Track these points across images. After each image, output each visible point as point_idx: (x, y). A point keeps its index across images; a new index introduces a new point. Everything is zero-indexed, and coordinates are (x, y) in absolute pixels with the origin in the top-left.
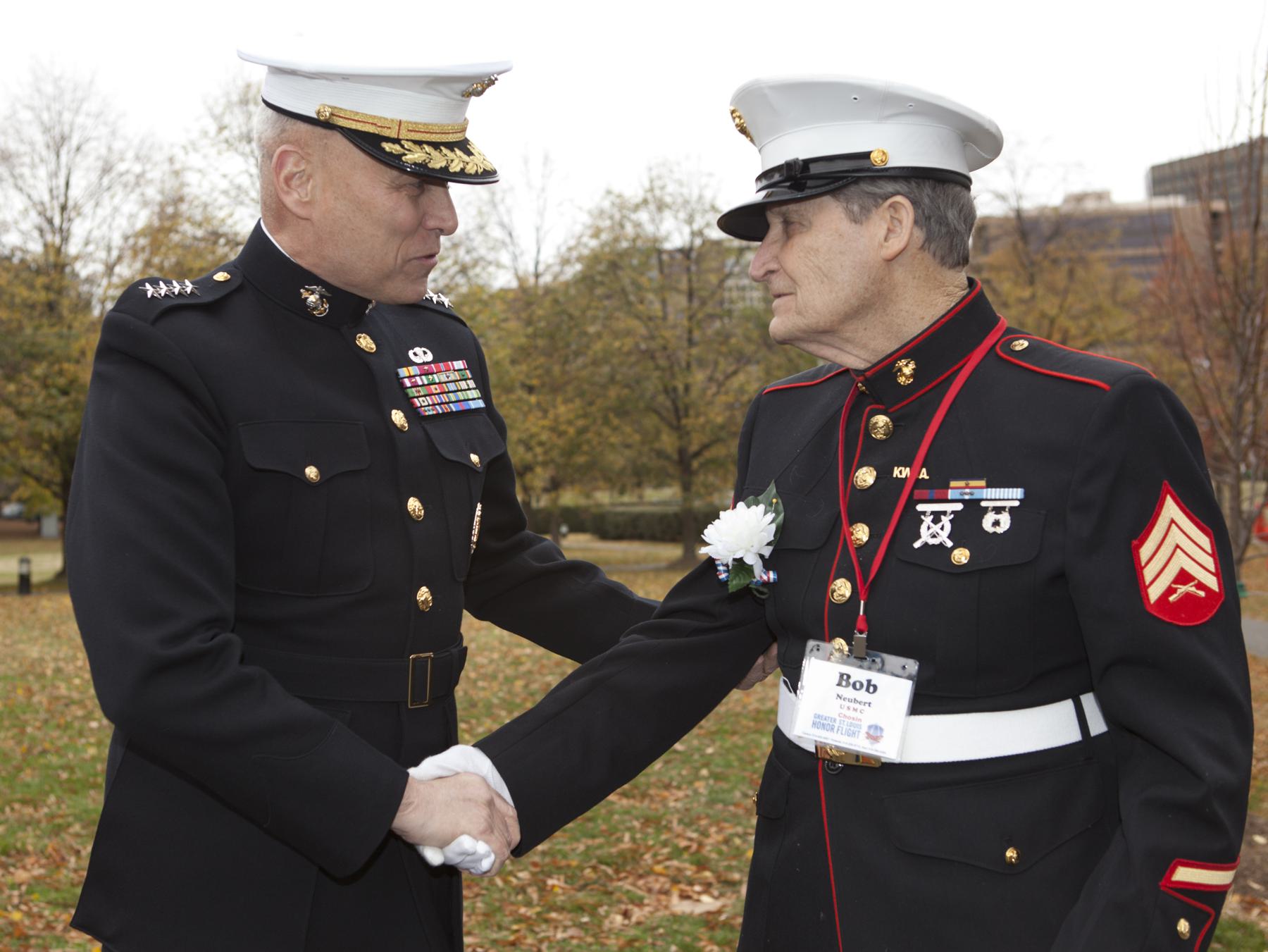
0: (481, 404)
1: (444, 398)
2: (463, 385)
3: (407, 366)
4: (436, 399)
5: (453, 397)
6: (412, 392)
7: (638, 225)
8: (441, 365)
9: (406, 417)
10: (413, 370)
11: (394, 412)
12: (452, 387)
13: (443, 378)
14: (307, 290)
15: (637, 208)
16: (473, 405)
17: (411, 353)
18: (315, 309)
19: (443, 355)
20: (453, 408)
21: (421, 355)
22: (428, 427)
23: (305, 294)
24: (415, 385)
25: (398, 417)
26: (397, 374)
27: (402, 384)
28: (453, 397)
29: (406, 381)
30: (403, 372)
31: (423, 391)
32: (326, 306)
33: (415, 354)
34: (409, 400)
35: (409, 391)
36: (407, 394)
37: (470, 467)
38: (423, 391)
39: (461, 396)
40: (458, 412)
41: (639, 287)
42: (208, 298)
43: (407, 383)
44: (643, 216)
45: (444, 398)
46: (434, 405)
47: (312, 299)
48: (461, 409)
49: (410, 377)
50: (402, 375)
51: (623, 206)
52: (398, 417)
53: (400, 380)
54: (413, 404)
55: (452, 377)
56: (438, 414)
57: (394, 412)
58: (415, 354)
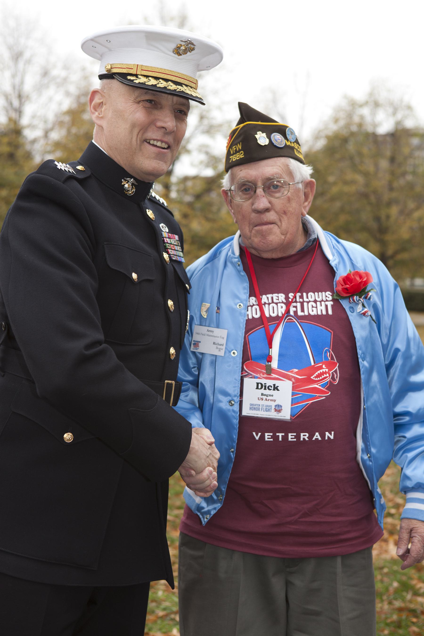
7: (362, 117)
15: (361, 106)
23: (124, 182)
41: (360, 154)
44: (366, 111)
47: (126, 186)
51: (354, 105)
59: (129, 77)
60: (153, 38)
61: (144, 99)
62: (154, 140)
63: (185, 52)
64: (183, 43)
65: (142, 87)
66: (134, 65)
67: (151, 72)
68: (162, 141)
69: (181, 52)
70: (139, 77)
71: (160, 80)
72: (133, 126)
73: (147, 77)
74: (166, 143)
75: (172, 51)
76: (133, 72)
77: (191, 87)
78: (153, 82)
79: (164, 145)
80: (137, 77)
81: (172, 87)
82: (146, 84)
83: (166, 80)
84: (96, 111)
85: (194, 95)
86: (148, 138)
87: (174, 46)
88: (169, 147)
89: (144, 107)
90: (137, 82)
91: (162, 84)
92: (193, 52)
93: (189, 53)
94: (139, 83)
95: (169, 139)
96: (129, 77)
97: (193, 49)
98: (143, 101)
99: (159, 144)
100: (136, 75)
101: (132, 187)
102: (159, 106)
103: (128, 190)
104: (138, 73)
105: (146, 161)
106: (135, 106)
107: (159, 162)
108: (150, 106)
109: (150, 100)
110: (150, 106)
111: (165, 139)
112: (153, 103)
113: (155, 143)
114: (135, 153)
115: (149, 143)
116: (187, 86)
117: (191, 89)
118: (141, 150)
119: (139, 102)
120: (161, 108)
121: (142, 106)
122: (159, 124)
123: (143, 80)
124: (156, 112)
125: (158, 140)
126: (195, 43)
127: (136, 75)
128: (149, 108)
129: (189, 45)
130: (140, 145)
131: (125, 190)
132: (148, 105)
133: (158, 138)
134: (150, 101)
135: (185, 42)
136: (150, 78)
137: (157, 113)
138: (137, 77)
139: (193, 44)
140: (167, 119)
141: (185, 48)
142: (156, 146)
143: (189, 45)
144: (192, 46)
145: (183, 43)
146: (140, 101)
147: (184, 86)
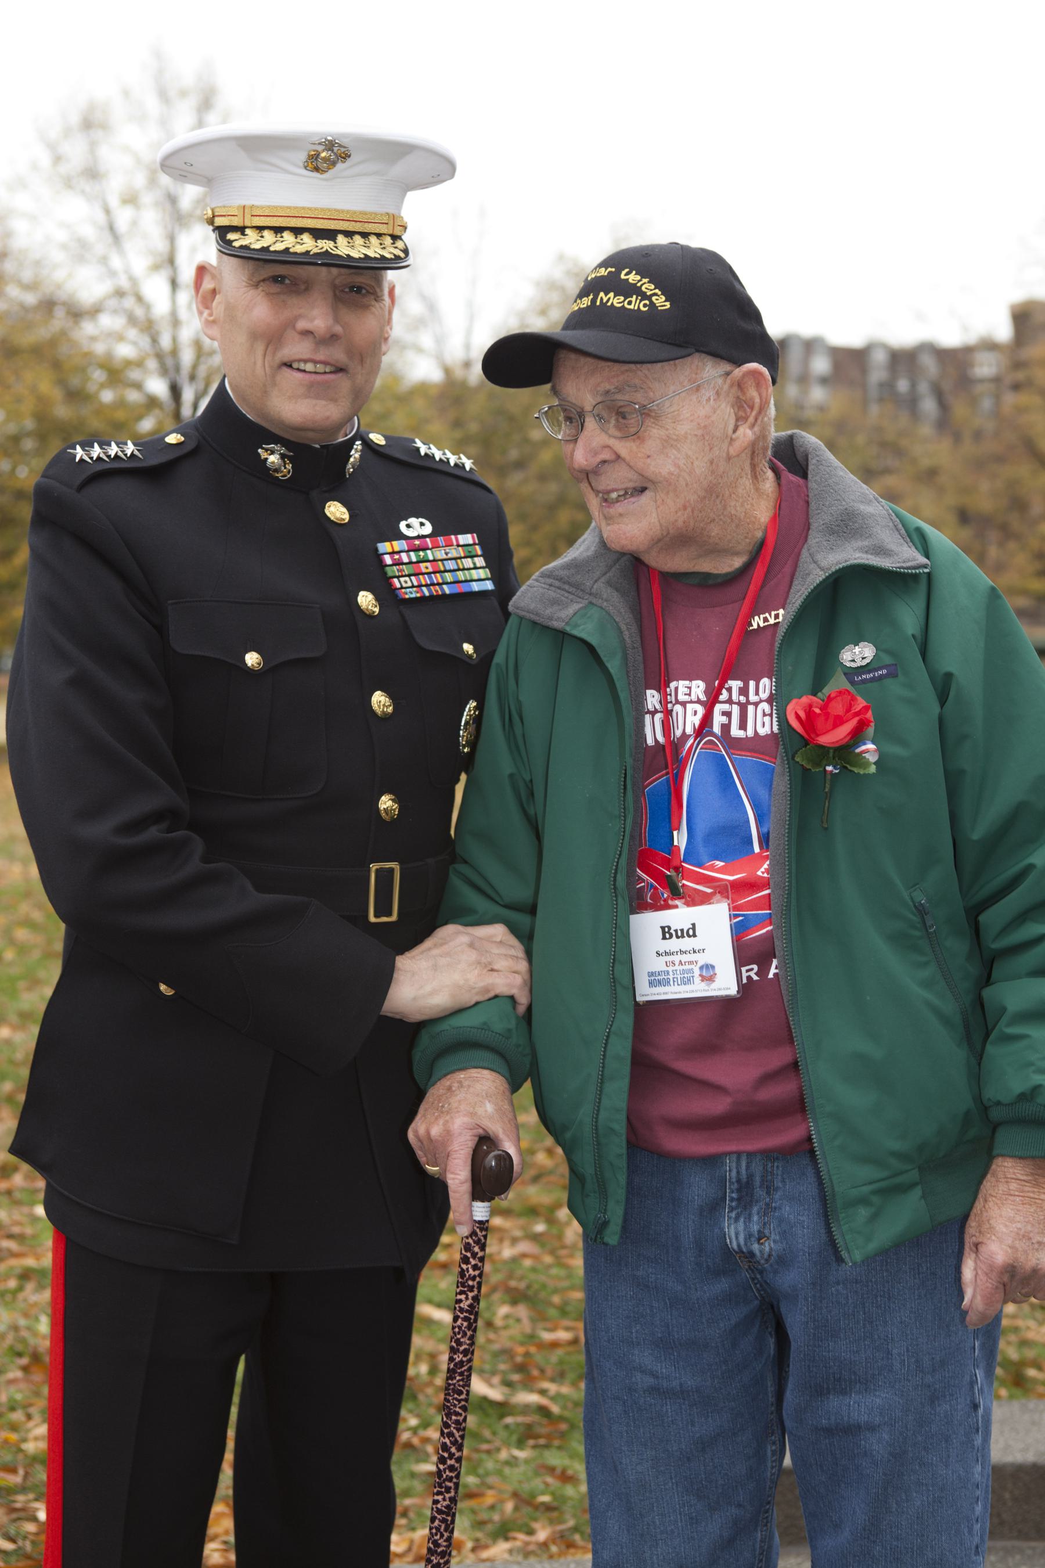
0: (489, 586)
2: (468, 563)
5: (449, 577)
9: (377, 599)
10: (398, 545)
12: (451, 565)
13: (440, 554)
16: (476, 587)
19: (444, 528)
20: (447, 589)
24: (399, 563)
25: (366, 600)
26: (377, 550)
28: (449, 577)
30: (384, 547)
31: (406, 570)
34: (387, 580)
35: (387, 568)
36: (386, 573)
38: (406, 570)
39: (461, 576)
40: (452, 596)
43: (388, 560)
52: (366, 600)
53: (379, 557)
54: (391, 585)
55: (453, 553)
59: (231, 236)
60: (258, 147)
61: (265, 276)
62: (299, 361)
64: (320, 148)
66: (238, 208)
67: (268, 219)
70: (248, 231)
72: (254, 336)
73: (260, 229)
74: (325, 363)
75: (301, 165)
76: (236, 222)
77: (365, 235)
78: (269, 239)
79: (320, 368)
80: (243, 234)
82: (252, 247)
83: (297, 231)
86: (286, 360)
87: (302, 156)
88: (340, 370)
89: (268, 294)
90: (236, 244)
91: (288, 240)
93: (340, 166)
94: (241, 247)
95: (338, 354)
97: (345, 156)
98: (264, 280)
99: (309, 367)
100: (241, 230)
104: (247, 224)
105: (293, 406)
106: (252, 292)
108: (279, 290)
109: (280, 276)
110: (279, 290)
111: (320, 356)
112: (287, 281)
113: (302, 366)
114: (265, 392)
115: (290, 366)
116: (349, 234)
117: (358, 240)
118: (274, 384)
119: (256, 286)
120: (307, 289)
121: (262, 294)
122: (302, 325)
123: (252, 240)
125: (305, 361)
126: (345, 142)
127: (241, 230)
128: (278, 293)
130: (273, 376)
132: (275, 288)
133: (305, 357)
134: (277, 279)
135: (320, 144)
136: (266, 233)
137: (296, 305)
138: (243, 234)
140: (316, 312)
141: (327, 156)
142: (304, 371)
143: (335, 149)
144: (343, 150)
145: (320, 148)
146: (259, 282)
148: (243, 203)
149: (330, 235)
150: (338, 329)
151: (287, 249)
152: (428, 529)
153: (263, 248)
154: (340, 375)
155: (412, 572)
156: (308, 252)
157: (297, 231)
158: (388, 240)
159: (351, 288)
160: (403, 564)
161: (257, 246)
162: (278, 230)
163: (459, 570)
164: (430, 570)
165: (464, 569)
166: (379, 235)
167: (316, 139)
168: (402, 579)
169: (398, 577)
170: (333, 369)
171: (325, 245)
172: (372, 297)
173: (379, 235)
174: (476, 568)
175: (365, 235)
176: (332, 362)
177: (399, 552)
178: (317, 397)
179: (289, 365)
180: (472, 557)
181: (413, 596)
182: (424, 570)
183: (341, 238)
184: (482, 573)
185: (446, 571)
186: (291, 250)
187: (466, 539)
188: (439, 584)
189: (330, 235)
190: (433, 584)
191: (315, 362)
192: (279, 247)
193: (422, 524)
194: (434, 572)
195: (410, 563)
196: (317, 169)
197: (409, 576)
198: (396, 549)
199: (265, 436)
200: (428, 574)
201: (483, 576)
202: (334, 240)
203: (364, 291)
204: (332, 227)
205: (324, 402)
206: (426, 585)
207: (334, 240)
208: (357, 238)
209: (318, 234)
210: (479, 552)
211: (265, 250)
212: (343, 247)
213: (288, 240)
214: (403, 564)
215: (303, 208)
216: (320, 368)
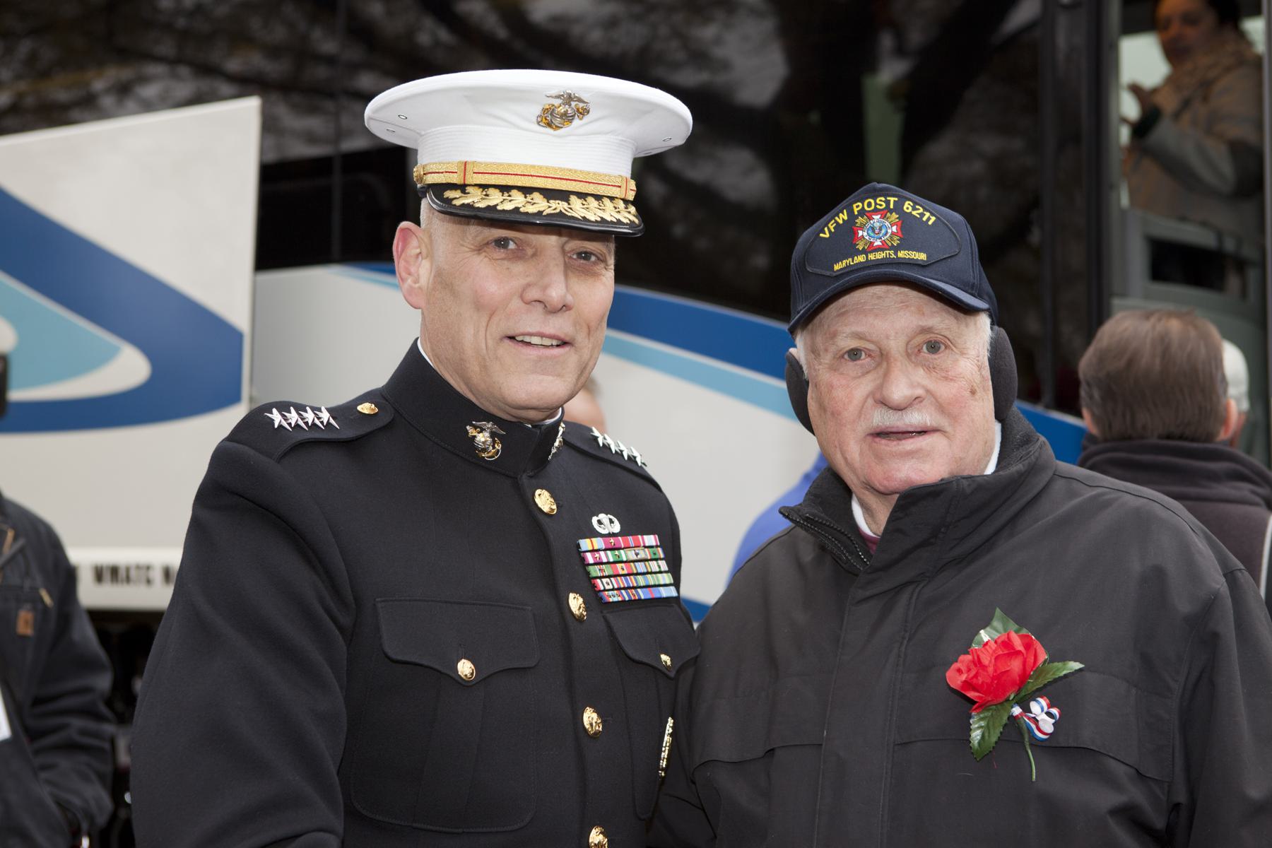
1: (632, 581)
2: (654, 566)
3: (590, 537)
4: (622, 582)
5: (641, 580)
6: (595, 571)
8: (630, 538)
10: (598, 543)
11: (572, 596)
12: (641, 567)
13: (631, 555)
14: (475, 427)
17: (595, 520)
18: (484, 450)
20: (642, 594)
21: (606, 523)
22: (610, 617)
23: (471, 431)
26: (578, 546)
27: (583, 559)
28: (641, 580)
29: (589, 555)
30: (585, 544)
31: (608, 570)
32: (498, 447)
33: (600, 522)
34: (590, 580)
35: (591, 569)
36: (588, 573)
37: (658, 670)
38: (608, 570)
39: (651, 580)
42: (349, 434)
43: (590, 558)
45: (632, 581)
46: (619, 589)
48: (649, 596)
49: (593, 551)
50: (583, 548)
53: (580, 556)
54: (594, 586)
55: (642, 555)
56: (624, 601)
57: (572, 596)
58: (600, 522)
59: (449, 194)
63: (567, 118)
64: (557, 102)
65: (470, 216)
68: (542, 335)
69: (557, 121)
70: (469, 189)
71: (514, 192)
73: (484, 187)
76: (455, 179)
77: (598, 198)
79: (547, 342)
81: (539, 205)
84: (410, 274)
85: (593, 219)
87: (537, 110)
88: (563, 343)
89: (491, 259)
92: (587, 118)
93: (576, 122)
96: (449, 194)
97: (583, 112)
98: (488, 243)
99: (535, 340)
100: (462, 188)
101: (494, 442)
102: (530, 251)
103: (484, 450)
107: (541, 377)
112: (512, 246)
113: (527, 339)
117: (592, 202)
120: (534, 255)
123: (475, 198)
124: (518, 268)
125: (531, 335)
126: (584, 97)
127: (462, 188)
129: (573, 104)
131: (476, 448)
132: (500, 253)
134: (501, 243)
135: (558, 97)
136: (491, 191)
138: (464, 192)
139: (580, 100)
143: (573, 104)
144: (581, 105)
145: (557, 102)
147: (573, 198)
148: (464, 159)
149: (564, 195)
150: (569, 299)
151: (517, 209)
152: (616, 528)
153: (489, 207)
154: (567, 349)
155: (612, 573)
156: (540, 213)
157: (526, 191)
158: (621, 205)
159: (579, 254)
160: (602, 563)
161: (482, 205)
162: (504, 189)
163: (648, 573)
164: (625, 572)
165: (652, 573)
166: (612, 199)
167: (554, 92)
168: (605, 580)
169: (600, 578)
170: (555, 343)
171: (558, 206)
172: (602, 265)
173: (612, 199)
174: (660, 572)
175: (598, 198)
176: (562, 336)
177: (598, 551)
178: (544, 372)
179: (512, 338)
180: (656, 560)
181: (616, 599)
182: (621, 572)
183: (573, 198)
184: (667, 578)
185: (638, 574)
186: (522, 210)
187: (651, 540)
188: (634, 588)
189: (564, 195)
190: (629, 588)
191: (542, 335)
192: (509, 206)
193: (611, 522)
194: (629, 575)
195: (608, 563)
196: (549, 125)
197: (609, 577)
198: (596, 547)
199: (477, 414)
200: (624, 575)
201: (668, 582)
202: (568, 201)
203: (593, 258)
204: (564, 188)
205: (550, 378)
206: (624, 588)
207: (568, 201)
208: (590, 199)
209: (549, 194)
210: (662, 556)
211: (492, 209)
212: (577, 209)
213: (518, 200)
214: (602, 563)
215: (533, 167)
216: (547, 342)
